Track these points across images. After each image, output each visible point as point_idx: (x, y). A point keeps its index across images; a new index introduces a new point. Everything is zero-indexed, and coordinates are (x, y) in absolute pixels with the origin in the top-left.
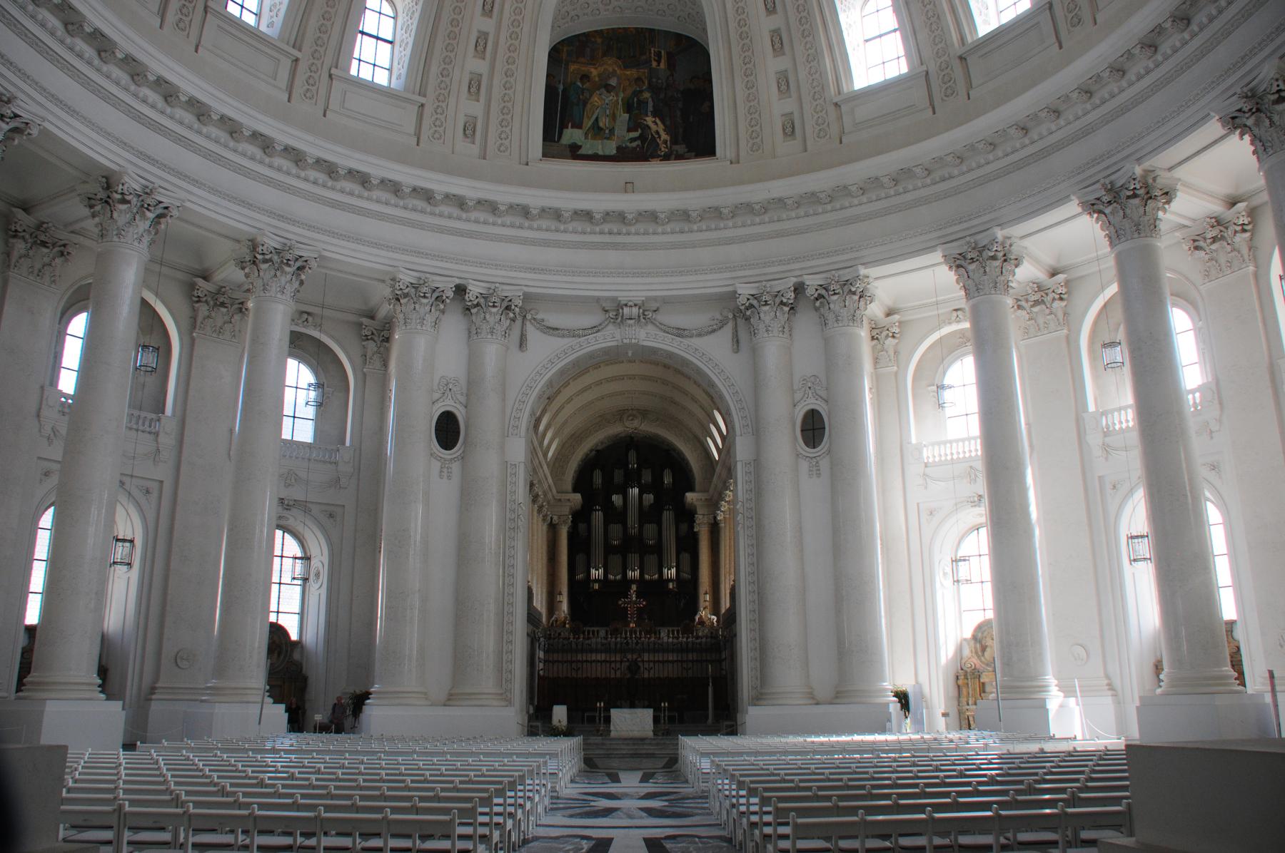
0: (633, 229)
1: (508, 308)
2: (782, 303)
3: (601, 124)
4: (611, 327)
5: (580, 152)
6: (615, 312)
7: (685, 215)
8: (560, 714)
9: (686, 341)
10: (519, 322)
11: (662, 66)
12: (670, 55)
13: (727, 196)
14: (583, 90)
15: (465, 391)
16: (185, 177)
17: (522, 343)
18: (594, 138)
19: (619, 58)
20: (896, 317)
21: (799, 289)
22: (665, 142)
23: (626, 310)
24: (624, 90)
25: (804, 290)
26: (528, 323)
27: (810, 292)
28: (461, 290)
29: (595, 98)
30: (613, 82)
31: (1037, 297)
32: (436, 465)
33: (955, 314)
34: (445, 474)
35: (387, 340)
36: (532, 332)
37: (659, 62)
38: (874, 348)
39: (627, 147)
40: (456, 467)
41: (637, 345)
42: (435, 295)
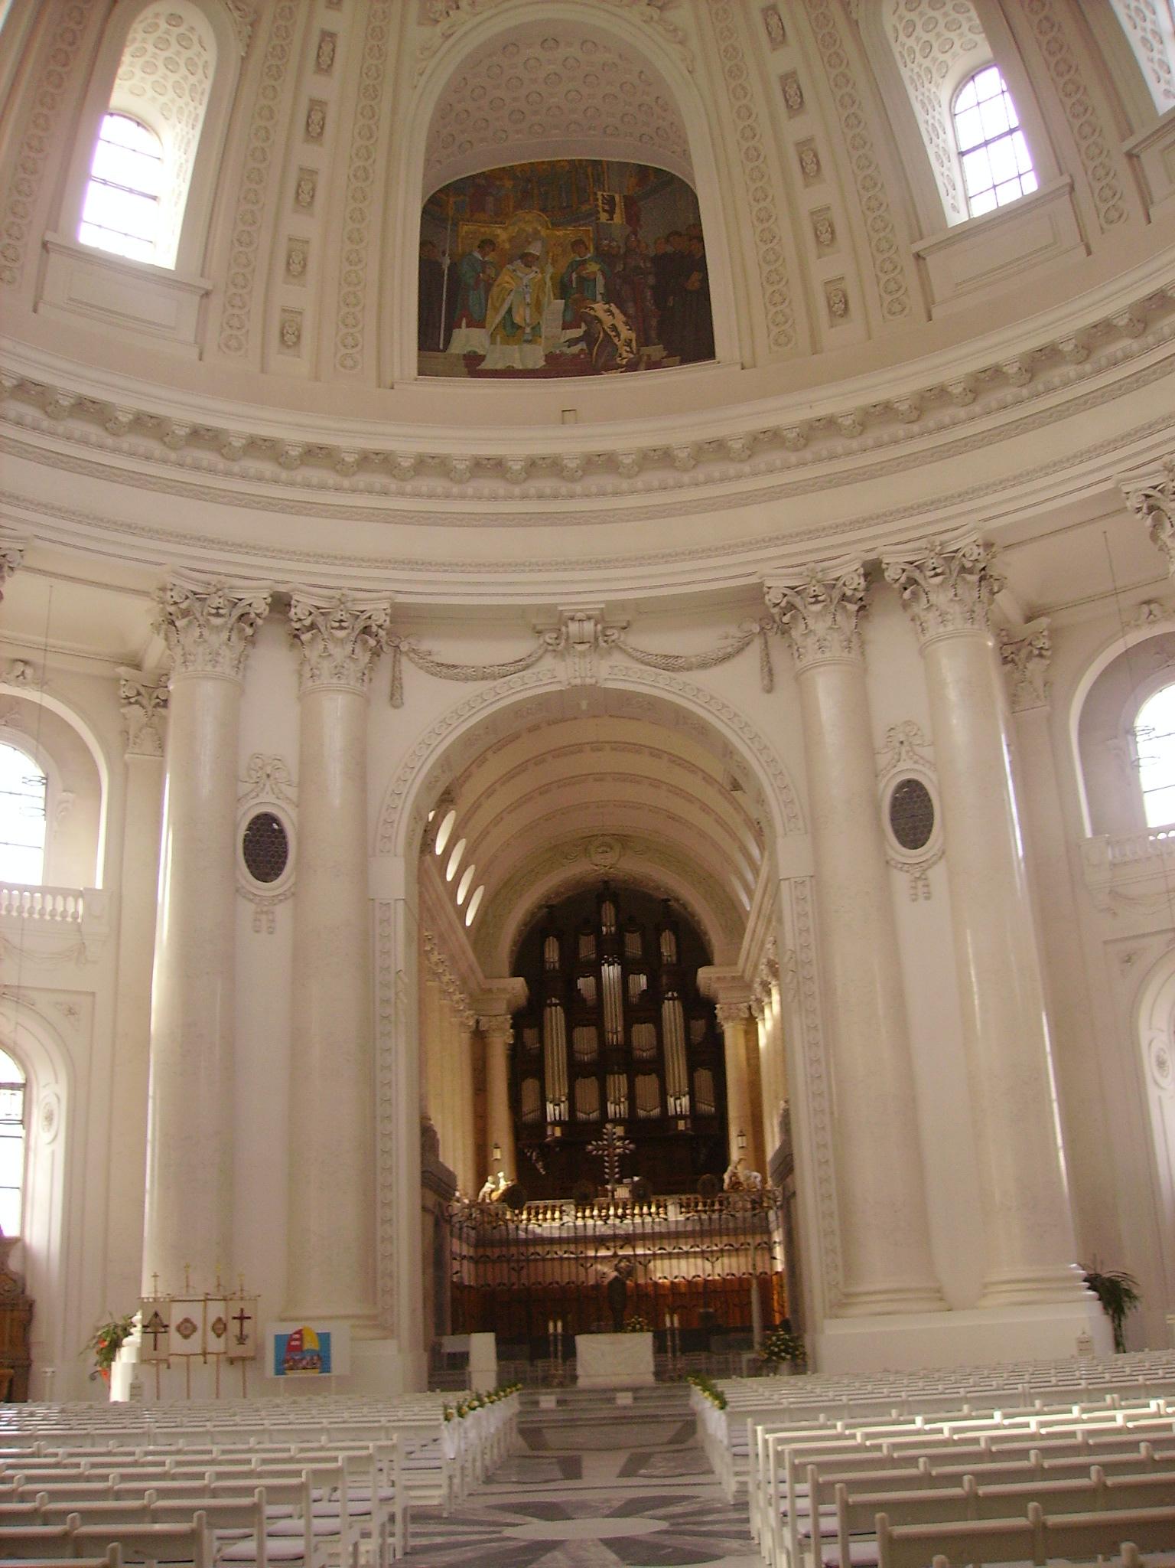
0: (578, 488)
1: (366, 630)
2: (844, 597)
3: (517, 320)
5: (484, 366)
6: (552, 628)
7: (664, 457)
8: (482, 1347)
11: (618, 218)
12: (630, 203)
13: (737, 422)
14: (484, 264)
15: (295, 778)
18: (506, 341)
19: (542, 210)
20: (1043, 622)
21: (873, 572)
22: (628, 343)
23: (573, 627)
24: (554, 262)
25: (883, 571)
26: (404, 659)
27: (890, 574)
28: (281, 603)
29: (505, 278)
30: (535, 249)
33: (1145, 609)
37: (611, 213)
39: (562, 354)
42: (236, 613)
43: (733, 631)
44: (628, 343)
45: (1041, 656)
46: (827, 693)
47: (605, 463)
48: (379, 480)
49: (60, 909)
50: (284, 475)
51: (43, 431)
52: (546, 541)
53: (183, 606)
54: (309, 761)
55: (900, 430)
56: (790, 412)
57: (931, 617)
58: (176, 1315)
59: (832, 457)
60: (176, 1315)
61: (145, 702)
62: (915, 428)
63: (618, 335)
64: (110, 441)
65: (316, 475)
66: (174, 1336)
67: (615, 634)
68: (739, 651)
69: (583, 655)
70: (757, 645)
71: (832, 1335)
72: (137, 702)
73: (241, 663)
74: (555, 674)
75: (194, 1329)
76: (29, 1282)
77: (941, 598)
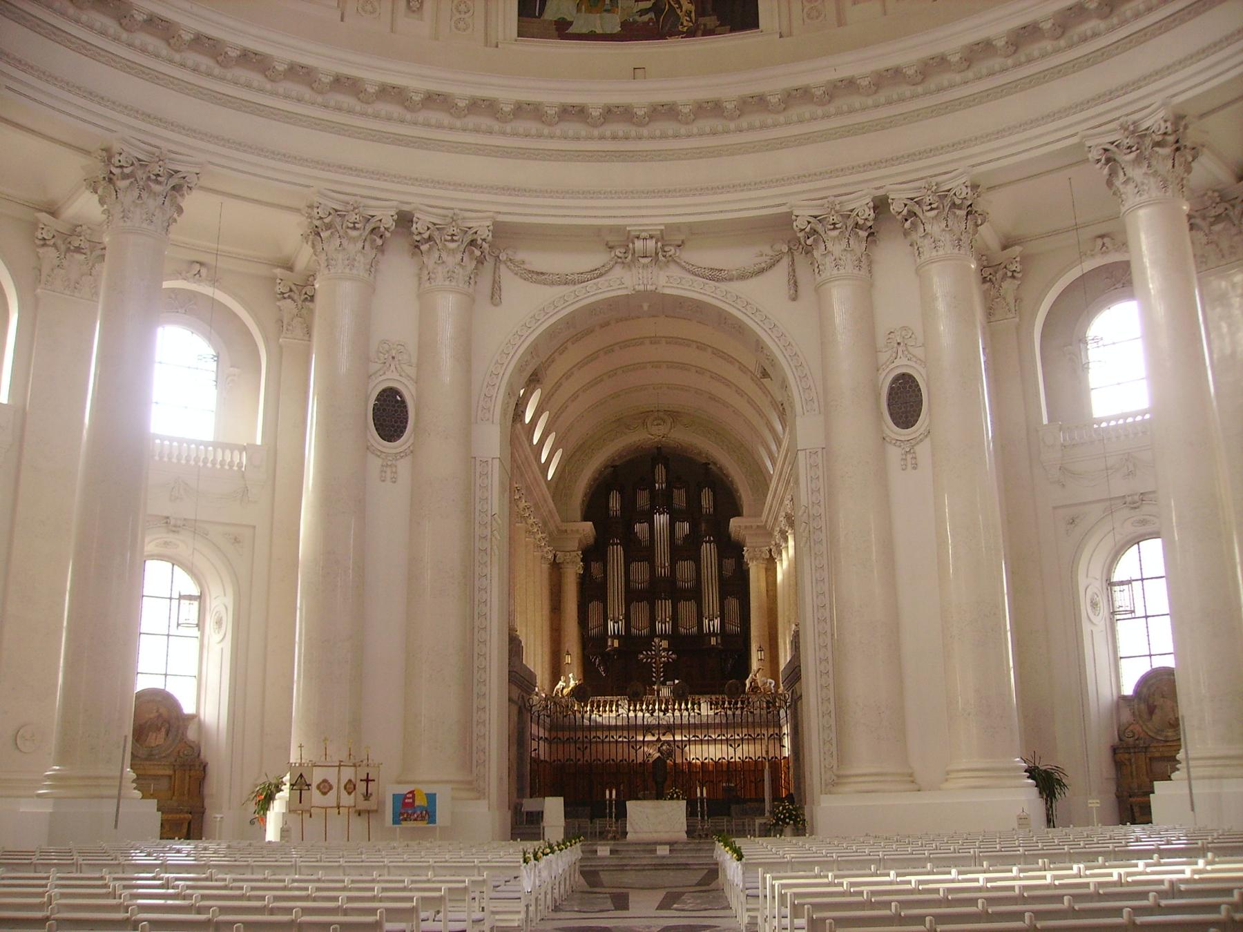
0: (645, 131)
1: (473, 243)
4: (618, 269)
5: (571, 30)
6: (621, 244)
7: (714, 108)
8: (553, 808)
9: (724, 286)
10: (489, 264)
13: (775, 81)
15: (414, 360)
17: (495, 295)
18: (589, 11)
20: (1017, 249)
21: (881, 205)
22: (689, 14)
23: (639, 244)
25: (889, 205)
26: (502, 267)
27: (895, 208)
28: (405, 220)
31: (1220, 210)
32: (375, 463)
33: (1099, 242)
34: (389, 475)
35: (312, 298)
36: (506, 276)
38: (985, 295)
39: (635, 22)
40: (403, 466)
41: (653, 292)
42: (369, 227)
43: (767, 250)
44: (689, 14)
45: (1013, 277)
46: (840, 301)
47: (668, 111)
48: (485, 122)
49: (228, 459)
50: (408, 116)
51: (215, 77)
52: (618, 174)
53: (327, 221)
54: (426, 347)
55: (906, 90)
56: (817, 74)
57: (927, 242)
58: (316, 777)
59: (851, 111)
60: (316, 777)
61: (296, 297)
62: (920, 89)
63: (681, 7)
64: (268, 86)
65: (434, 116)
66: (315, 793)
67: (671, 250)
68: (771, 266)
69: (645, 266)
70: (786, 261)
71: (825, 807)
72: (289, 297)
73: (372, 267)
74: (624, 282)
75: (331, 788)
77: (935, 229)
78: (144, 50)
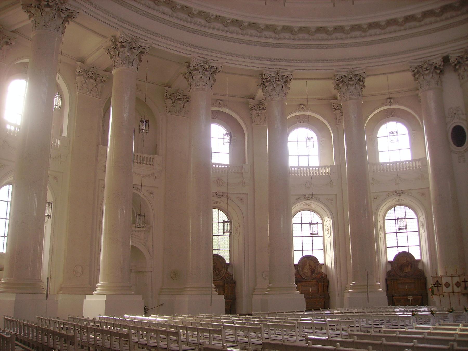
16: (293, 61)
28: (446, 60)
42: (433, 67)
49: (414, 165)
51: (364, 37)
58: (444, 281)
60: (444, 281)
64: (383, 31)
66: (444, 288)
75: (449, 285)
76: (327, 277)
78: (337, 39)
